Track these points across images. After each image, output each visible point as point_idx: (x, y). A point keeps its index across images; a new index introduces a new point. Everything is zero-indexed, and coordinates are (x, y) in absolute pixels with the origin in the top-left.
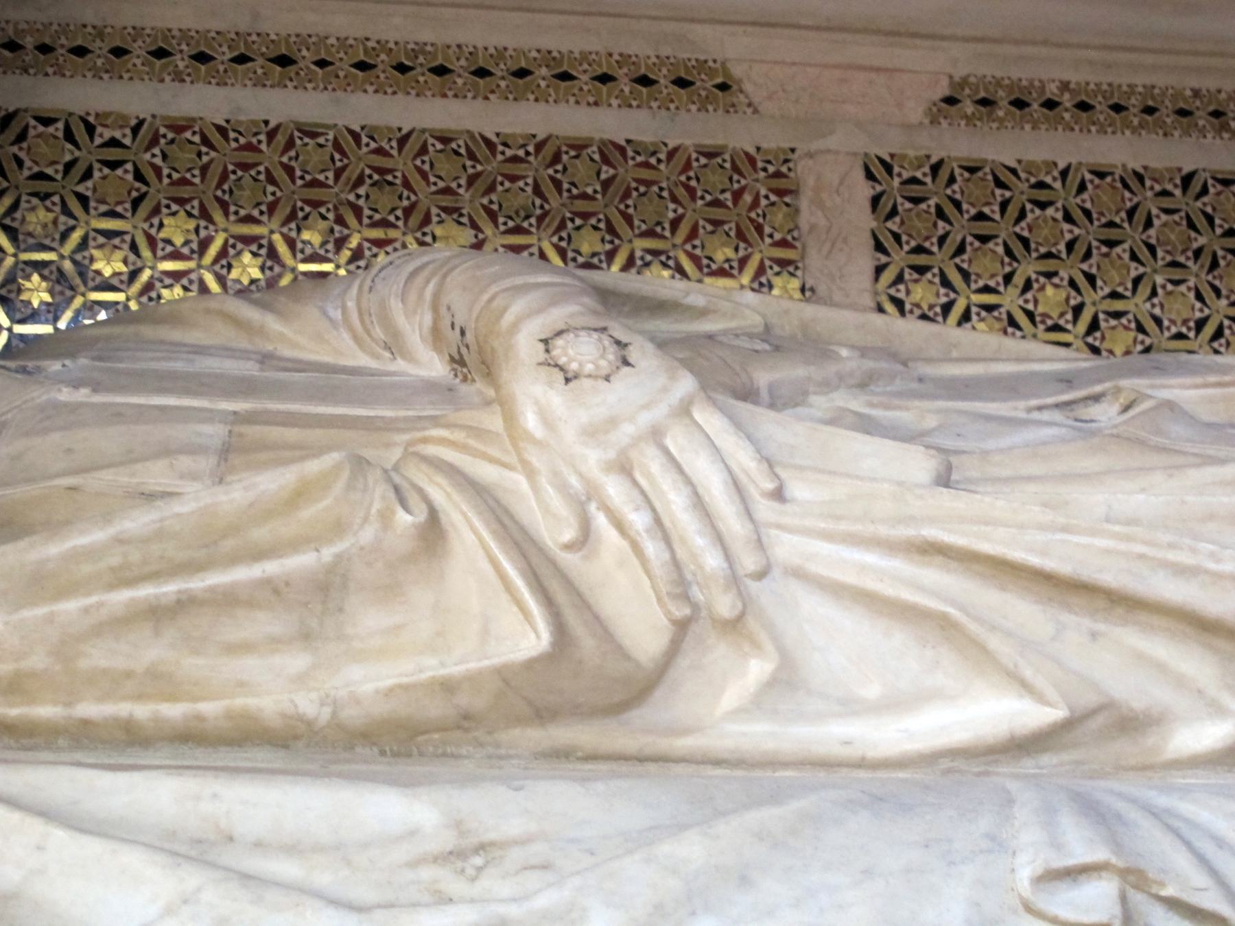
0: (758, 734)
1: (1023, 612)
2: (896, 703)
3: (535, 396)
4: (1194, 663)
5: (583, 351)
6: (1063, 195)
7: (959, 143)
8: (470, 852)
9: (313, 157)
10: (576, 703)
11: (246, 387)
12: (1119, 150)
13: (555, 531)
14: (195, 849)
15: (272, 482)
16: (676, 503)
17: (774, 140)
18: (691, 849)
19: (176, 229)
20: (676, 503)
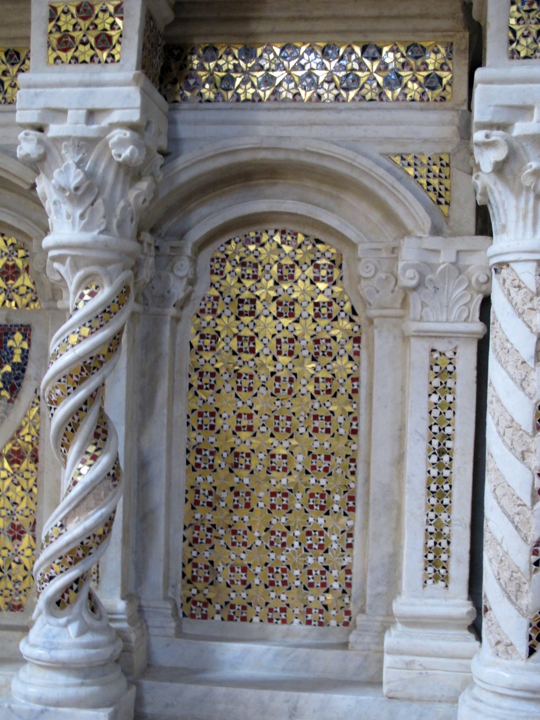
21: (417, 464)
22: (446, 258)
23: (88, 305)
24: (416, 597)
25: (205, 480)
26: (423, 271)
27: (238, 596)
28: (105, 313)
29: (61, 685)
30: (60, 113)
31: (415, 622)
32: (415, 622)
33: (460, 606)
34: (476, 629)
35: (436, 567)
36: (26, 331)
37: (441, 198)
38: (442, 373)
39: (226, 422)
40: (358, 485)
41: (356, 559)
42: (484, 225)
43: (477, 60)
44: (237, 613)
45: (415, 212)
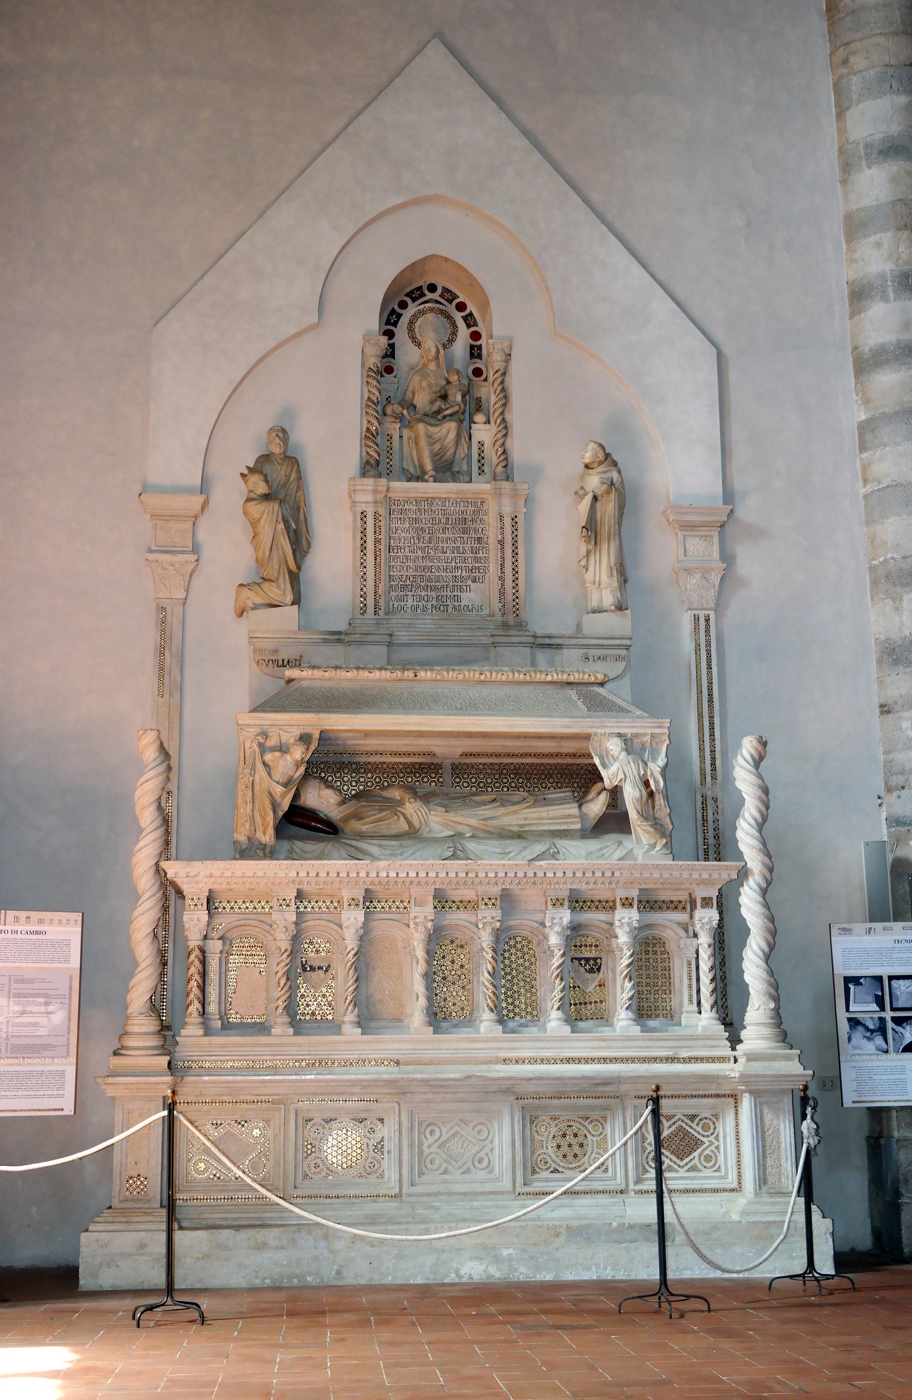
0: (427, 835)
1: (452, 824)
2: (440, 832)
3: (407, 804)
4: (467, 829)
5: (412, 800)
6: (476, 767)
7: (463, 761)
8: (401, 846)
9: (385, 766)
10: (412, 834)
11: (380, 802)
12: (483, 760)
13: (410, 818)
14: (380, 846)
15: (384, 814)
16: (420, 815)
17: (439, 761)
18: (419, 846)
19: (370, 775)
20: (420, 815)
21: (686, 981)
22: (689, 943)
23: (629, 953)
24: (687, 1007)
25: (641, 989)
26: (685, 945)
27: (649, 1013)
28: (631, 956)
29: (631, 1022)
30: (623, 918)
31: (688, 1012)
32: (688, 1012)
33: (695, 1008)
34: (700, 1013)
35: (691, 1001)
36: (601, 959)
37: (687, 931)
38: (689, 964)
39: (644, 976)
40: (672, 988)
41: (672, 1004)
42: (695, 935)
43: (693, 908)
44: (649, 1017)
45: (682, 933)
